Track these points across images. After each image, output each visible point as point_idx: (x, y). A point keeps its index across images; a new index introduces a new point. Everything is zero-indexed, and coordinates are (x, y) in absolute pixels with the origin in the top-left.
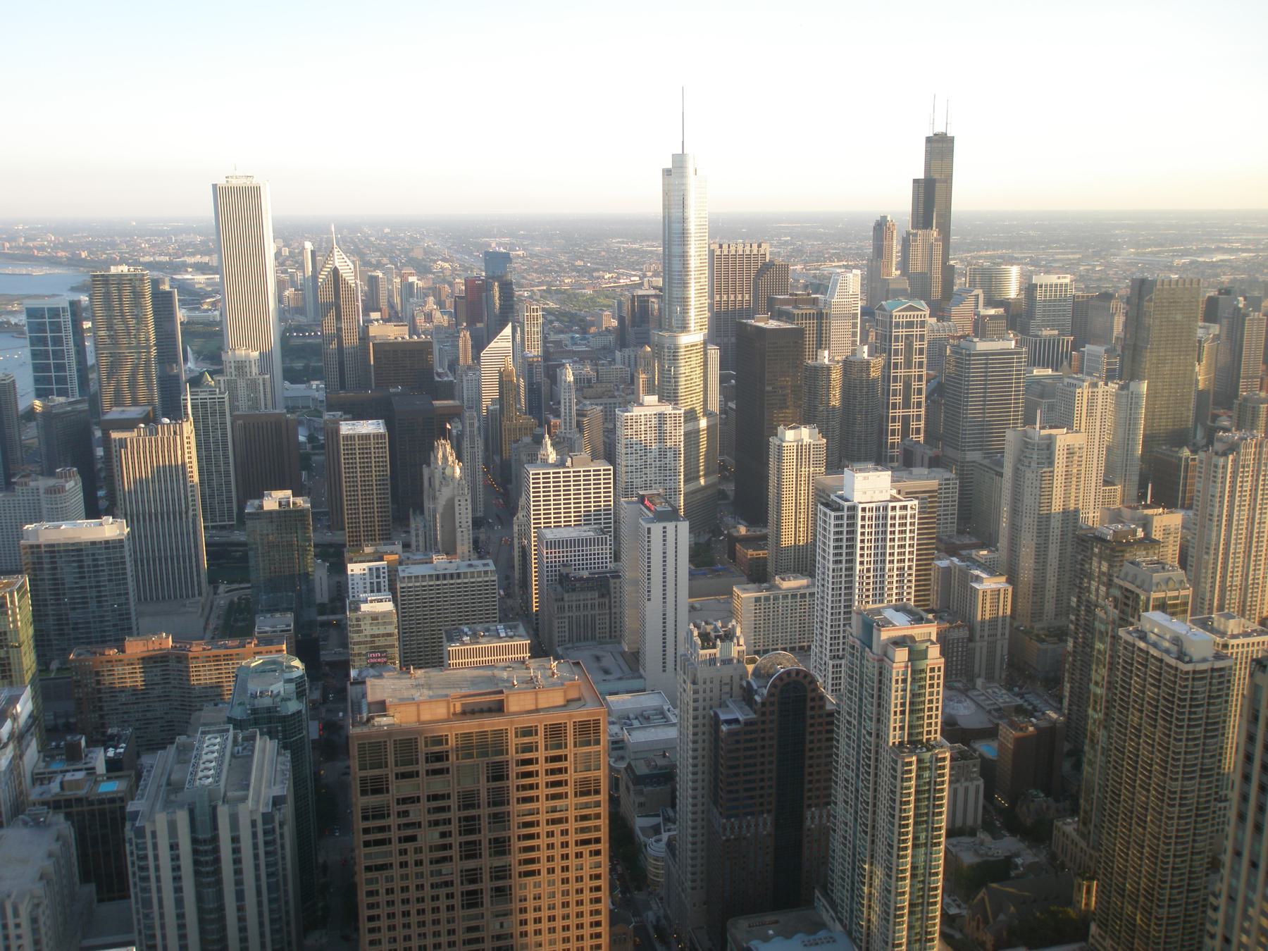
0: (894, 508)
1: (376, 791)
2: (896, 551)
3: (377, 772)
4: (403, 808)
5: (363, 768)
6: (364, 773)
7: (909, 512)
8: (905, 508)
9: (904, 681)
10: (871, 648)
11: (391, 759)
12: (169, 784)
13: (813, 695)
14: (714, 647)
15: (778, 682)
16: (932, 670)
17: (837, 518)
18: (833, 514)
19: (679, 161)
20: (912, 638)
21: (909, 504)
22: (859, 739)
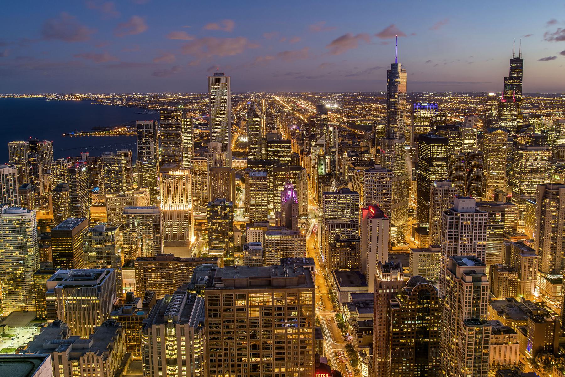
0: (476, 216)
1: (215, 316)
2: (477, 235)
3: (216, 307)
4: (226, 324)
5: (210, 305)
6: (210, 307)
7: (484, 218)
8: (482, 215)
9: (470, 291)
10: (455, 275)
11: (222, 303)
12: (159, 313)
13: (433, 296)
14: (390, 272)
15: (417, 289)
16: (484, 287)
17: (450, 219)
18: (448, 217)
19: (394, 66)
20: (474, 272)
21: (484, 214)
22: (450, 317)
